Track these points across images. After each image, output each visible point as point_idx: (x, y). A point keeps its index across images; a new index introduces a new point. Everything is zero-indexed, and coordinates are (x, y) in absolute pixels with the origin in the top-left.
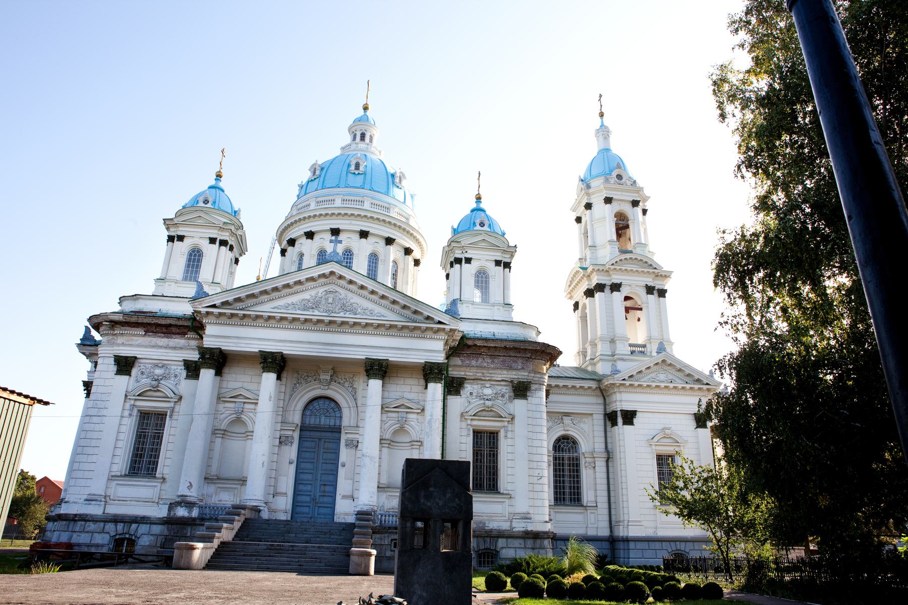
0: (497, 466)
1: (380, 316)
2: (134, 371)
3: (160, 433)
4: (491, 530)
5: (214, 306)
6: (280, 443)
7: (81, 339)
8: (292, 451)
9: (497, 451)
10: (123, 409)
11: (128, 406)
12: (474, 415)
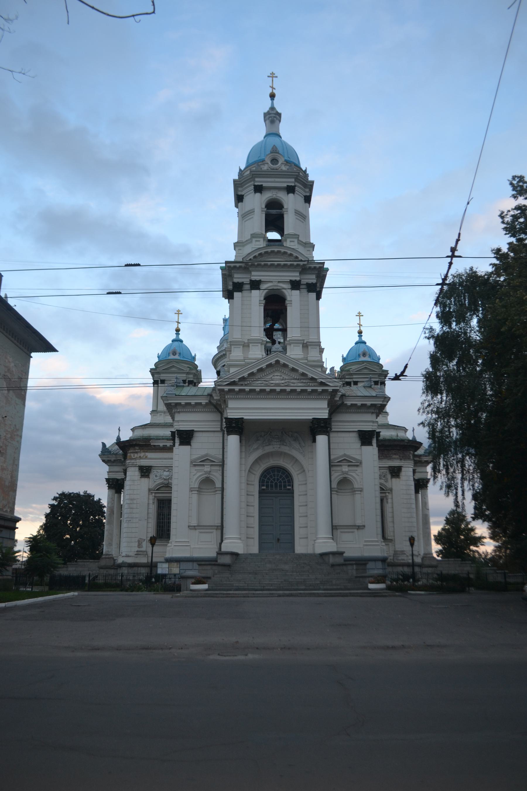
2: (152, 475)
7: (101, 452)
10: (149, 499)
11: (151, 497)
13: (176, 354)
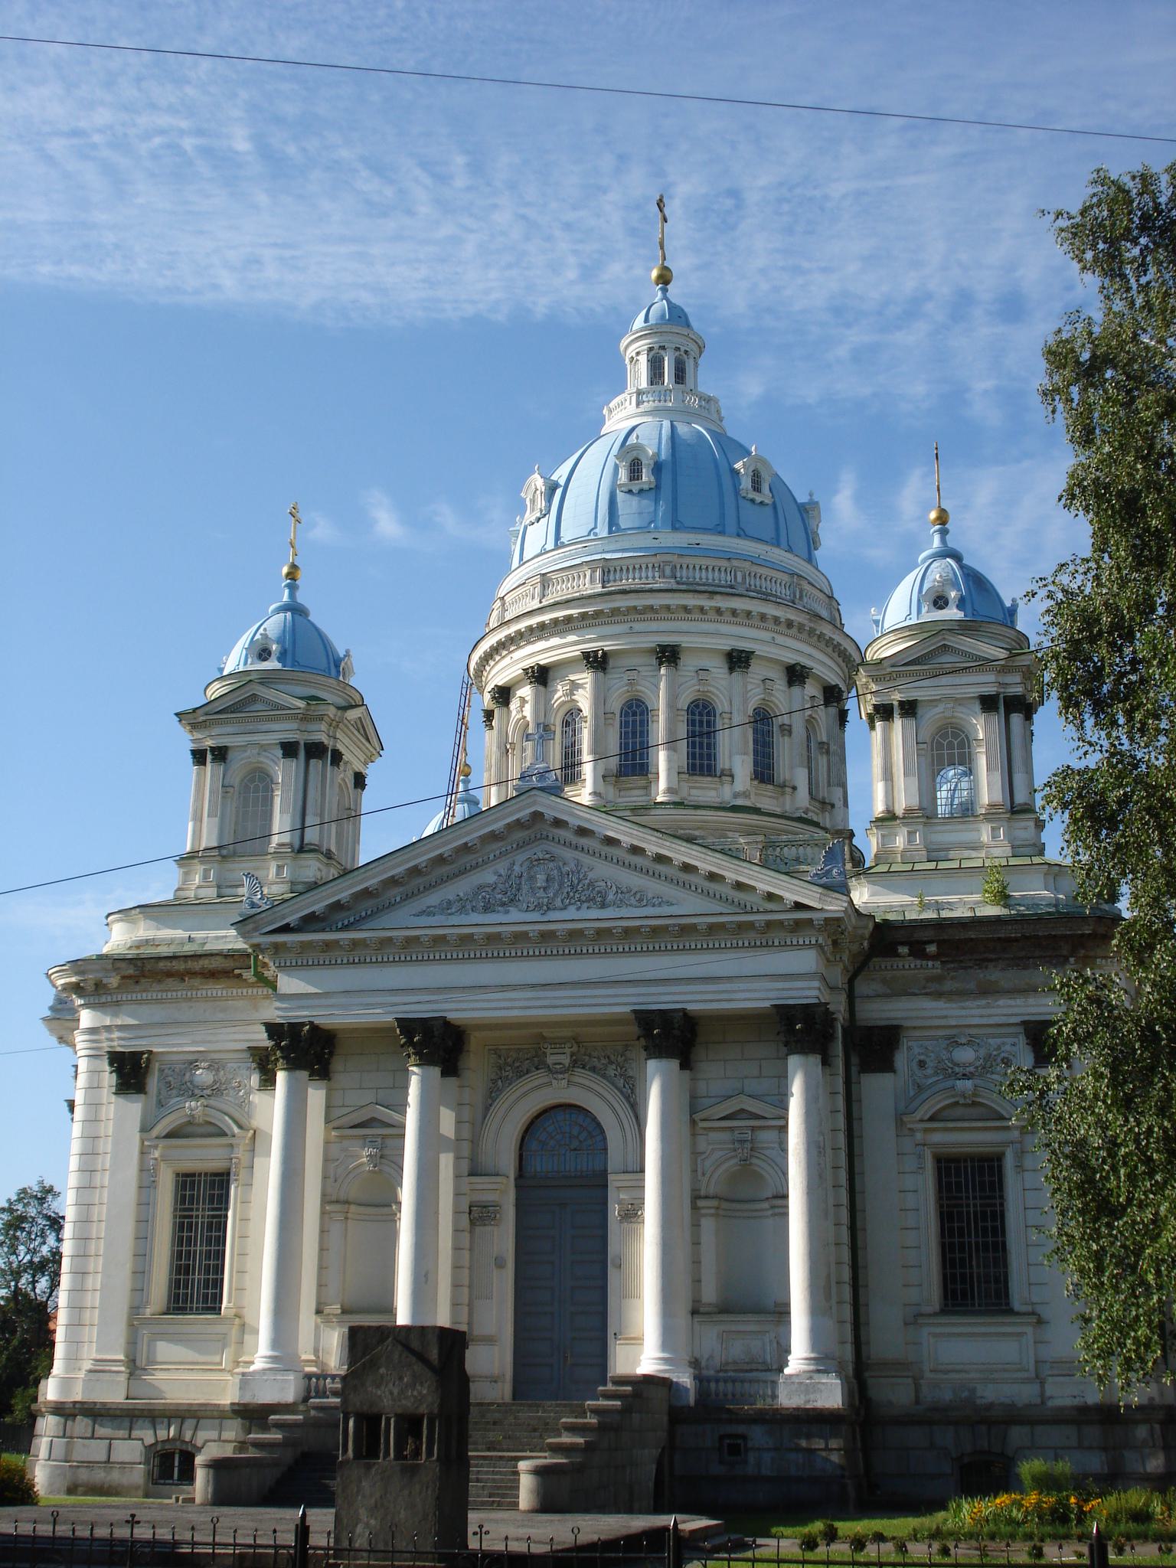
0: (1004, 1244)
1: (660, 905)
2: (153, 1082)
3: (219, 1216)
4: (990, 1406)
5: (286, 929)
6: (472, 1223)
8: (503, 1238)
9: (1002, 1205)
12: (932, 1119)
13: (270, 654)
